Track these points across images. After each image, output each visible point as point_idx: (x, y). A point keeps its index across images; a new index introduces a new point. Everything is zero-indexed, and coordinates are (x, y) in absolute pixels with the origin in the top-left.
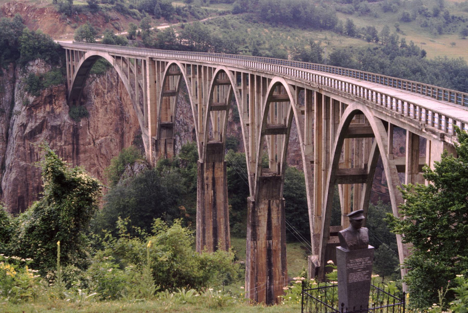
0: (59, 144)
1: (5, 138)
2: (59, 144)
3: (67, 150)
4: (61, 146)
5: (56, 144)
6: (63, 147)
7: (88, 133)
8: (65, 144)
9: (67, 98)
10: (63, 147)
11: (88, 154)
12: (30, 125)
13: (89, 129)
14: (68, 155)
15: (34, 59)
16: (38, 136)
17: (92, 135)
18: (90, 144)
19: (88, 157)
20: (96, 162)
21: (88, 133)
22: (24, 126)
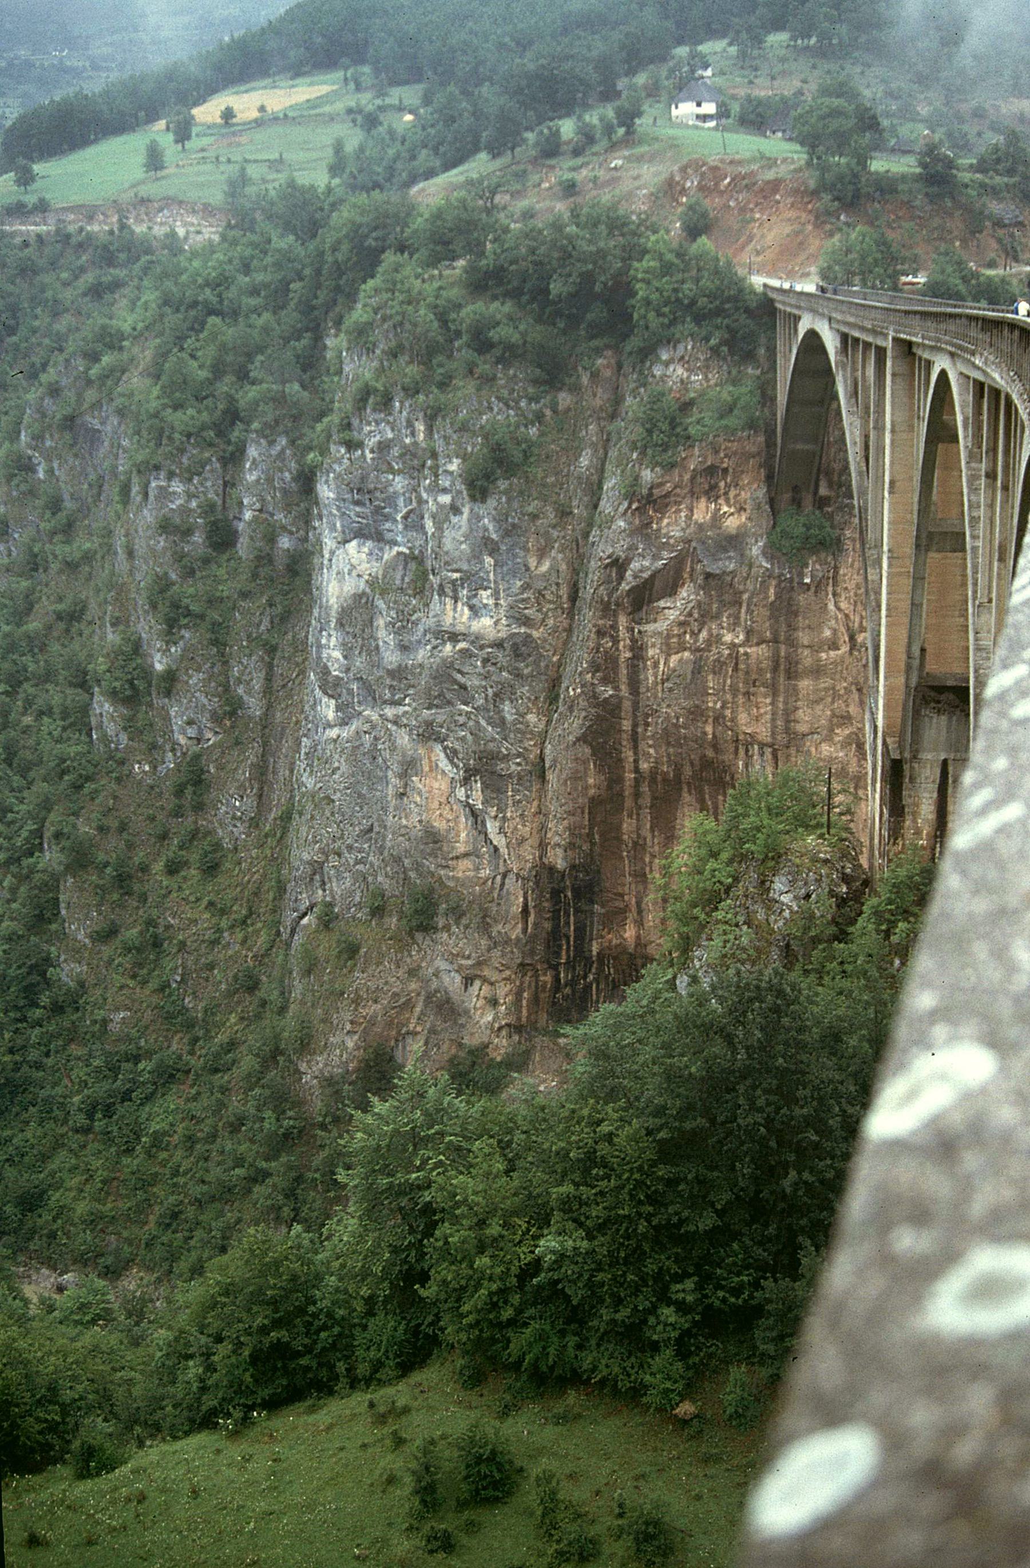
0: (728, 638)
1: (565, 598)
2: (728, 638)
3: (752, 661)
4: (733, 646)
5: (718, 639)
6: (741, 650)
7: (831, 606)
8: (746, 642)
9: (769, 478)
10: (741, 650)
11: (825, 682)
12: (635, 565)
13: (834, 595)
14: (754, 676)
15: (671, 341)
16: (662, 603)
17: (847, 616)
18: (834, 646)
19: (826, 689)
20: (853, 710)
21: (831, 606)
22: (618, 565)
